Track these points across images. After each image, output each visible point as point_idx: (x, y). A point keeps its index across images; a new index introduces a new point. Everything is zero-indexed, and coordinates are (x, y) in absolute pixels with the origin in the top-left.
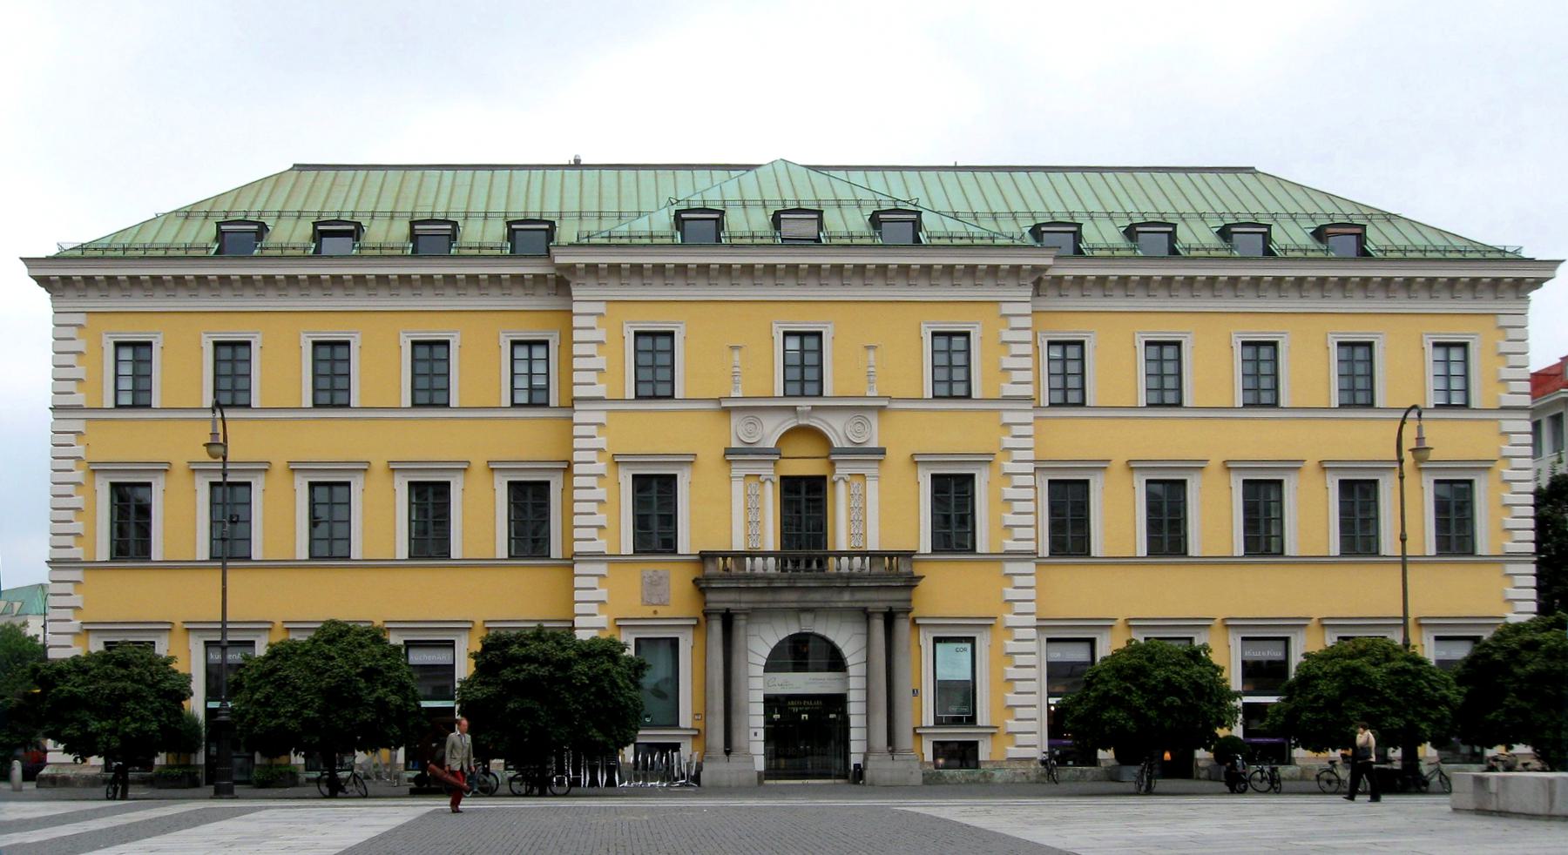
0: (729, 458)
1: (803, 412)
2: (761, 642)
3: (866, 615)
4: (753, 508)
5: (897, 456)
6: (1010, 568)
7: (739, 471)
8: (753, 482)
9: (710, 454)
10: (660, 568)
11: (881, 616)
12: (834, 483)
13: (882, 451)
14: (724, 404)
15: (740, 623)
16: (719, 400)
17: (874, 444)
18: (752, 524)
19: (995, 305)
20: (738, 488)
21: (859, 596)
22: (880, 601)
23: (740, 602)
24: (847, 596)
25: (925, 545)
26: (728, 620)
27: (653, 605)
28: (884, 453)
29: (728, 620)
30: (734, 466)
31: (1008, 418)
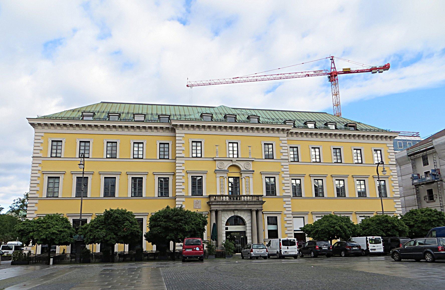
0: (216, 172)
1: (234, 161)
2: (225, 217)
3: (251, 211)
4: (222, 185)
5: (257, 172)
6: (285, 199)
7: (218, 175)
8: (222, 178)
9: (211, 171)
10: (199, 200)
11: (255, 211)
12: (242, 179)
13: (254, 171)
14: (214, 159)
15: (220, 213)
16: (213, 158)
17: (251, 169)
18: (222, 188)
20: (218, 179)
21: (249, 206)
22: (254, 207)
23: (220, 208)
24: (246, 206)
25: (265, 194)
26: (217, 212)
27: (197, 209)
28: (254, 172)
29: (217, 212)
30: (217, 174)
31: (283, 164)
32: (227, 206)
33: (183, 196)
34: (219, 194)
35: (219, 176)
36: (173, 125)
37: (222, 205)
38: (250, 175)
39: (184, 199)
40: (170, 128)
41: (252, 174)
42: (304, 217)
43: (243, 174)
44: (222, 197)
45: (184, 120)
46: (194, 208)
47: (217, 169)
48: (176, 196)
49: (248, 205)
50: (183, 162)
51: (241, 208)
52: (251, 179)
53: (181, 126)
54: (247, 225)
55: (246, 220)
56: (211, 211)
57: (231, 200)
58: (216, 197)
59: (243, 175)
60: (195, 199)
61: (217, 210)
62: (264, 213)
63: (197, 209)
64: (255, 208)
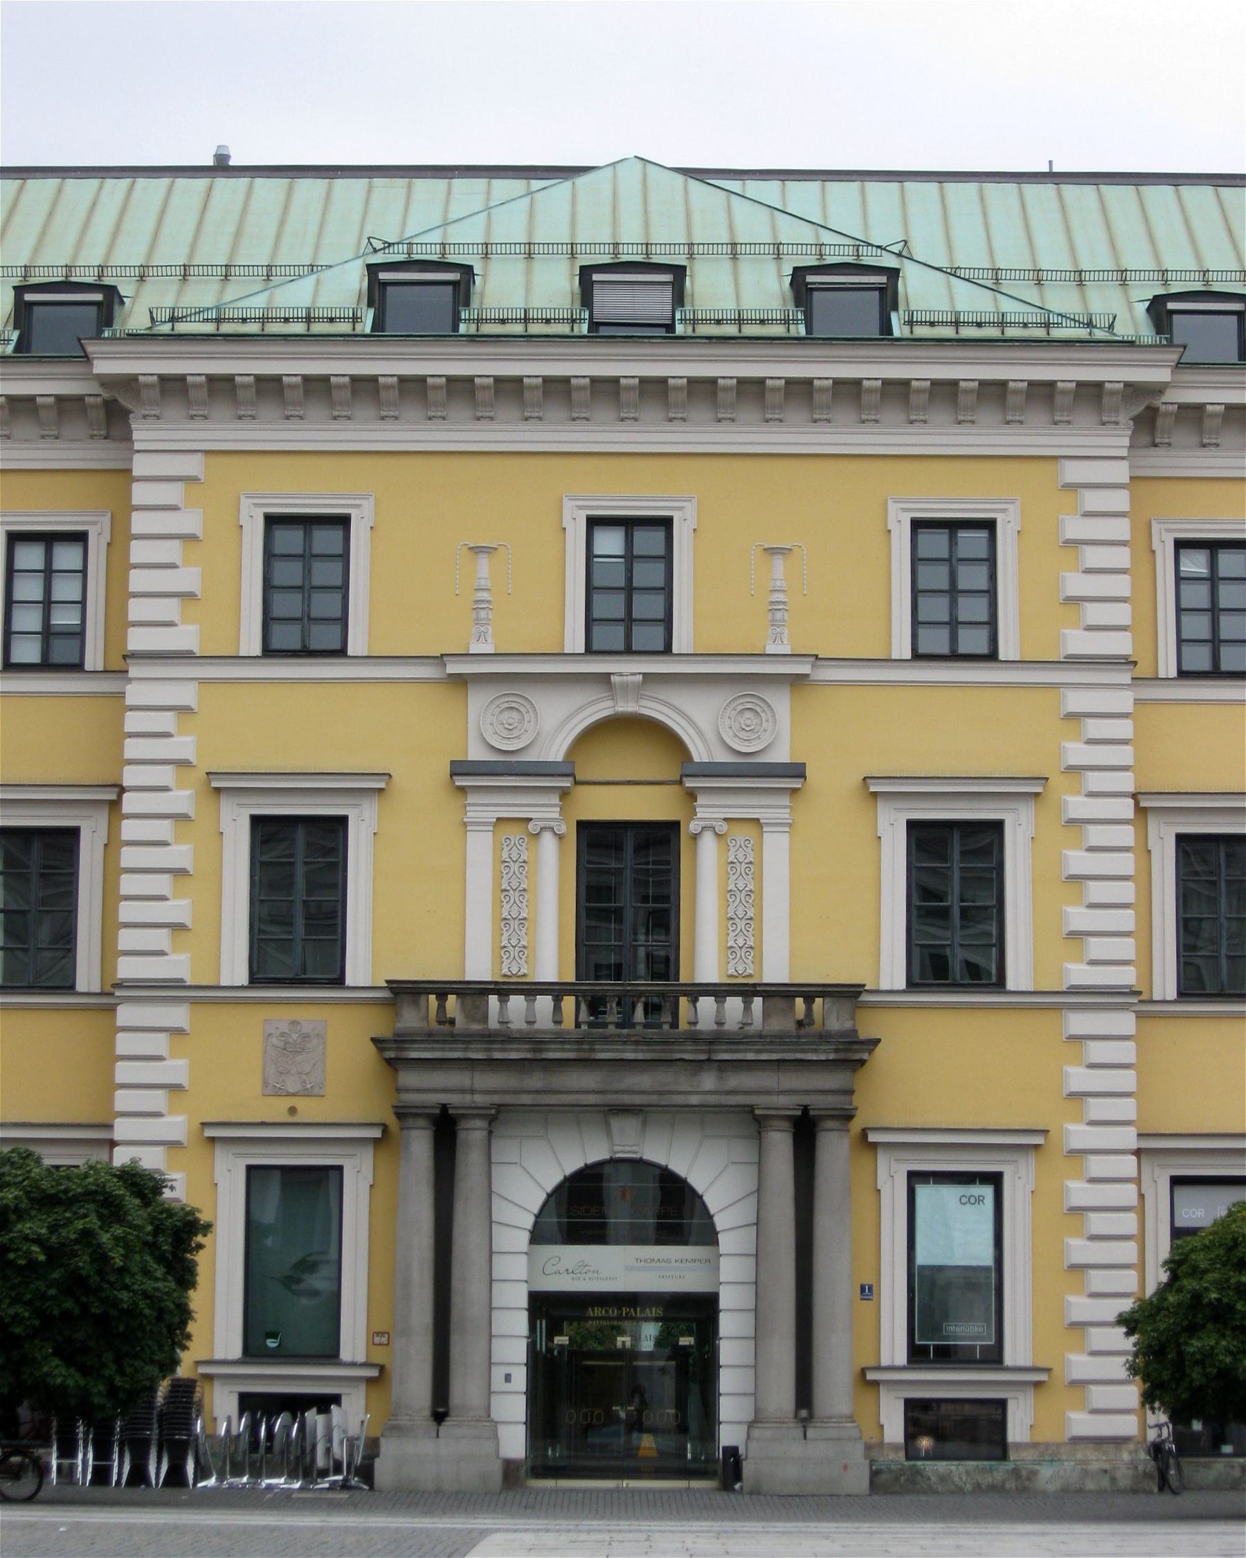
0: (461, 782)
1: (625, 687)
6: (1079, 1023)
7: (484, 809)
8: (515, 834)
10: (308, 1017)
11: (785, 1125)
12: (695, 837)
13: (797, 771)
14: (453, 668)
15: (472, 1135)
16: (441, 659)
17: (781, 755)
19: (1048, 467)
20: (480, 846)
23: (472, 1091)
24: (708, 1081)
30: (471, 799)
31: (1076, 701)
32: (536, 1080)
33: (178, 984)
34: (479, 969)
35: (492, 815)
36: (108, 382)
37: (491, 1064)
38: (771, 810)
39: (177, 1015)
40: (95, 407)
41: (785, 800)
42: (994, 1179)
43: (701, 800)
44: (432, 998)
45: (209, 328)
46: (265, 1083)
47: (476, 753)
48: (119, 985)
49: (720, 1070)
50: (185, 695)
51: (661, 1093)
52: (776, 847)
53: (173, 386)
54: (726, 1242)
55: (713, 1202)
56: (403, 1113)
57: (659, 1026)
58: (809, 998)
59: (710, 810)
60: (282, 1017)
61: (444, 1107)
62: (873, 1138)
63: (290, 1102)
64: (783, 1100)
